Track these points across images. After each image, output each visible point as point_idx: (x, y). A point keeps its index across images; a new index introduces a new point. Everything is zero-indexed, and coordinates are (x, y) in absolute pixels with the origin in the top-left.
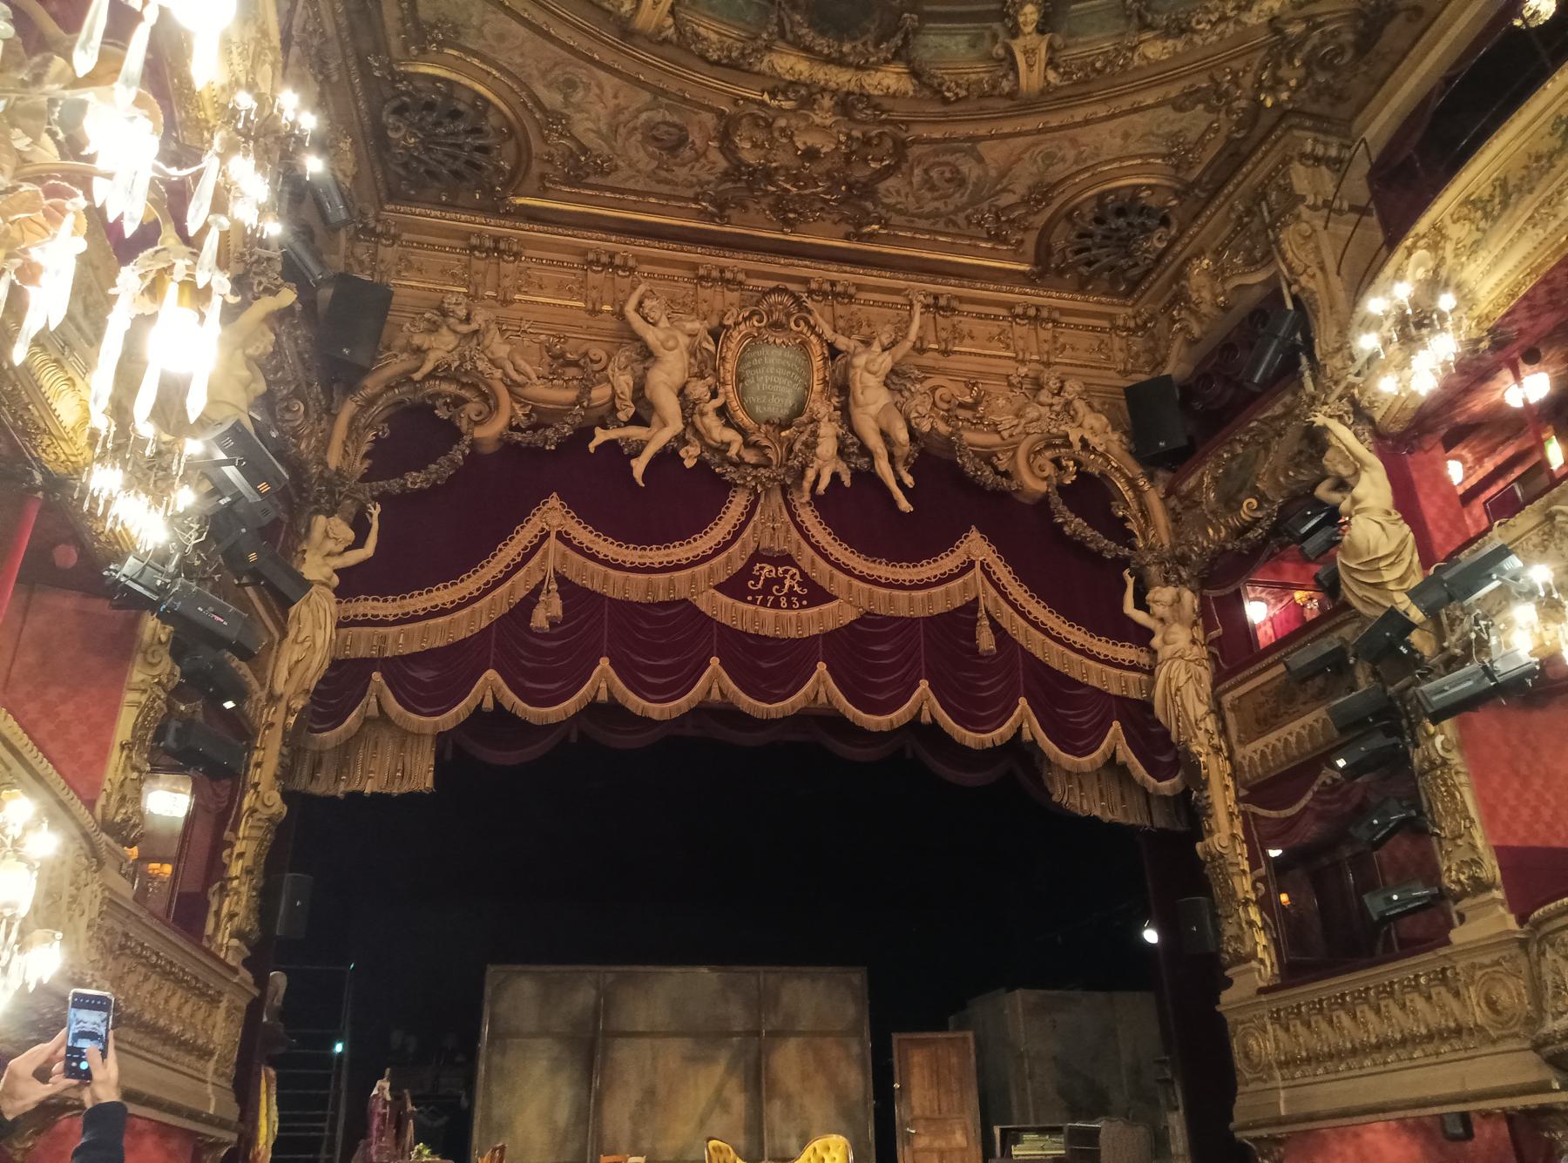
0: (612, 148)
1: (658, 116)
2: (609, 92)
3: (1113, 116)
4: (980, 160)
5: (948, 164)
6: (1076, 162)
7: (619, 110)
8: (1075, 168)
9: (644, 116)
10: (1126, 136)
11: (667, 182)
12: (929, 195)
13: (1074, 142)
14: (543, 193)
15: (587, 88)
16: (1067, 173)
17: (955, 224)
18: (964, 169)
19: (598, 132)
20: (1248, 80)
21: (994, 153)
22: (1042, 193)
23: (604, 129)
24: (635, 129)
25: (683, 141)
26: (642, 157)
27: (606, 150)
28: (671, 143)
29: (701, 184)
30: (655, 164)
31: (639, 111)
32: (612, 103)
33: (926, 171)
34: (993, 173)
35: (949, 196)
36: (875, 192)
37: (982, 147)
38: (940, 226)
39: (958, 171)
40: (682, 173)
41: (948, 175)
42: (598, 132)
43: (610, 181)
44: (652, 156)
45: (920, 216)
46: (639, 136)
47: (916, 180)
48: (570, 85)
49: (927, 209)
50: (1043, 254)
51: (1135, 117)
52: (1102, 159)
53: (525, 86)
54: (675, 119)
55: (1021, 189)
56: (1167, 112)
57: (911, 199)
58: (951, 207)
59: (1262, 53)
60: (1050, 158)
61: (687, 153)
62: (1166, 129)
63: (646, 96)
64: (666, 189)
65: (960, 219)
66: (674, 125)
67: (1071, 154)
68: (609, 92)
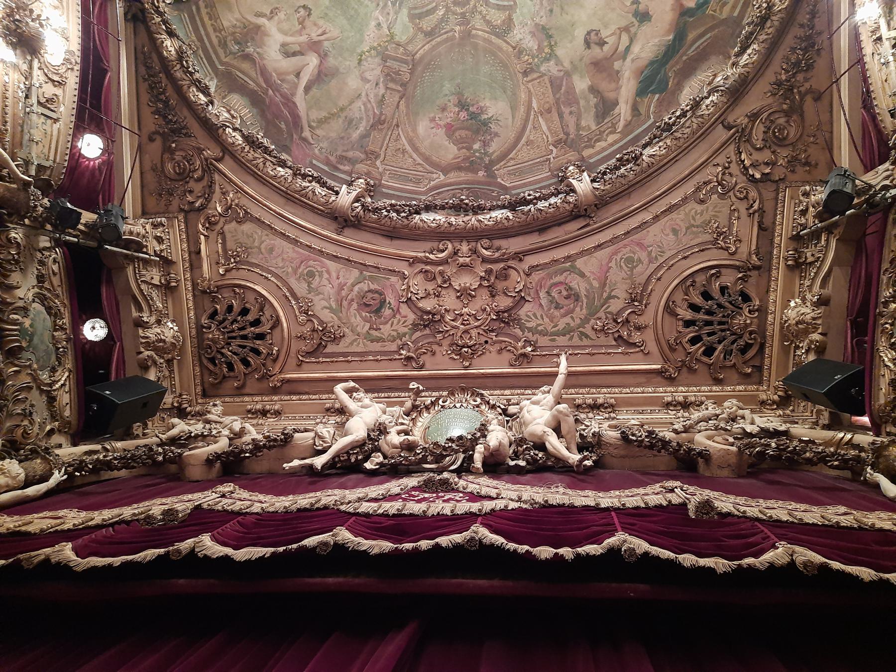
0: (340, 319)
2: (334, 275)
3: (656, 218)
4: (582, 275)
5: (561, 283)
6: (650, 262)
7: (341, 287)
9: (356, 288)
10: (675, 232)
11: (378, 340)
12: (557, 313)
13: (640, 245)
15: (321, 276)
16: (648, 272)
17: (587, 336)
18: (574, 284)
19: (330, 308)
20: (735, 169)
22: (638, 298)
24: (352, 300)
25: (383, 303)
26: (358, 321)
27: (337, 322)
28: (374, 305)
29: (400, 336)
30: (368, 325)
31: (353, 285)
32: (336, 283)
34: (596, 284)
35: (572, 311)
37: (579, 263)
38: (576, 341)
39: (571, 289)
41: (565, 293)
42: (330, 308)
43: (341, 347)
44: (365, 320)
45: (558, 334)
46: (355, 305)
47: (544, 302)
48: (311, 275)
49: (561, 326)
51: (674, 215)
52: (668, 254)
55: (621, 293)
56: (693, 207)
57: (546, 320)
58: (578, 321)
59: (731, 149)
60: (629, 260)
61: (387, 312)
62: (699, 220)
63: (355, 273)
64: (376, 347)
65: (588, 330)
66: (376, 292)
67: (643, 256)
68: (334, 275)
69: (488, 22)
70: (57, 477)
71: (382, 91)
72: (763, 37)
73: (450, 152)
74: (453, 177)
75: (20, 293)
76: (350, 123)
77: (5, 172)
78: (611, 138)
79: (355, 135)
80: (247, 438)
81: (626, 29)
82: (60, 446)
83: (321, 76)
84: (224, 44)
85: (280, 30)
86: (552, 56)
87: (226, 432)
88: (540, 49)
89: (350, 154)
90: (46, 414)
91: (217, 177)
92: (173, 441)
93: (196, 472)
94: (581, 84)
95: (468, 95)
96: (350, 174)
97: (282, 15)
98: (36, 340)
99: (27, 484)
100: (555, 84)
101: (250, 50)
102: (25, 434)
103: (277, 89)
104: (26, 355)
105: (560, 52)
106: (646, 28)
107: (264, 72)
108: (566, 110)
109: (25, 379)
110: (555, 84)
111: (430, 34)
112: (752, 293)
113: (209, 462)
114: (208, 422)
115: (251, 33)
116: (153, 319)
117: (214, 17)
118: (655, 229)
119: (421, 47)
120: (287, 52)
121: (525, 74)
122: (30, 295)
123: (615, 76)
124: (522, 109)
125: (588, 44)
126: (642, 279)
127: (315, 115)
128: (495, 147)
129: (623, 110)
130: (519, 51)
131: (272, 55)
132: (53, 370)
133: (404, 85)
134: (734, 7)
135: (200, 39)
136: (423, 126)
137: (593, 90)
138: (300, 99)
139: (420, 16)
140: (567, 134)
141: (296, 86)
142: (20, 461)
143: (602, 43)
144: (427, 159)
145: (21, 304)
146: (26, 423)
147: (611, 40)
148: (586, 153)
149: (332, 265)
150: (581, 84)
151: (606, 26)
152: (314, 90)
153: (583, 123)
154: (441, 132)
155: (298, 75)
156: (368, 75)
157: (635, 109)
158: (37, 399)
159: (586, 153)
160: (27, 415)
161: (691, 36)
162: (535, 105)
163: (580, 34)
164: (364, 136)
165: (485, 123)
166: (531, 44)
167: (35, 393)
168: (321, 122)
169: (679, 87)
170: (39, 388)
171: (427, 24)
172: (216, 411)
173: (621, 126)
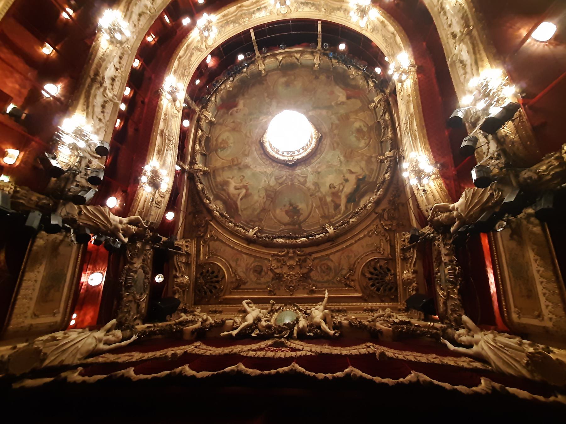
1: (256, 264)
3: (356, 242)
4: (332, 261)
6: (355, 256)
7: (247, 264)
8: (355, 259)
9: (253, 265)
10: (362, 246)
12: (324, 275)
14: (230, 293)
18: (329, 264)
20: (380, 226)
21: (334, 258)
22: (352, 269)
23: (244, 270)
25: (262, 270)
26: (253, 277)
28: (258, 271)
29: (268, 282)
33: (320, 267)
34: (337, 264)
36: (310, 277)
37: (331, 257)
38: (331, 285)
40: (263, 280)
43: (247, 286)
46: (252, 270)
49: (325, 279)
50: (364, 289)
51: (362, 241)
53: (228, 262)
54: (259, 264)
56: (367, 238)
58: (331, 278)
59: (378, 220)
61: (263, 273)
64: (259, 286)
65: (335, 281)
69: (299, 181)
70: (135, 337)
71: (265, 200)
72: (383, 187)
73: (286, 219)
74: (287, 227)
75: (135, 265)
76: (254, 210)
77: (140, 225)
78: (339, 216)
79: (256, 213)
80: (208, 323)
81: (342, 184)
82: (138, 324)
83: (246, 196)
84: (217, 186)
85: (235, 182)
86: (319, 191)
87: (200, 320)
88: (315, 188)
89: (254, 219)
90: (135, 312)
91: (209, 226)
92: (181, 323)
93: (187, 337)
94: (329, 199)
95: (293, 201)
96: (253, 225)
97: (235, 178)
98: (137, 283)
99: (122, 340)
100: (321, 199)
101: (225, 188)
102: (126, 320)
103: (232, 199)
104: (134, 288)
105: (321, 190)
106: (348, 184)
107: (228, 194)
108: (324, 207)
109: (130, 298)
110: (321, 199)
111: (281, 184)
112: (391, 268)
113: (193, 332)
114: (194, 315)
115: (226, 183)
116: (180, 275)
117: (215, 178)
118: (355, 245)
119: (278, 188)
120: (236, 188)
121: (311, 196)
122: (139, 266)
123: (340, 197)
124: (310, 207)
125: (330, 188)
126: (353, 262)
127: (243, 207)
128: (302, 218)
129: (343, 207)
130: (309, 189)
131: (231, 189)
132: (141, 294)
133: (272, 198)
134: (374, 178)
135: (210, 185)
136: (278, 211)
137: (332, 201)
138: (239, 203)
139: (278, 179)
140: (325, 214)
141: (238, 198)
142: (122, 331)
143: (335, 187)
144: (279, 221)
145: (135, 269)
146: (127, 315)
147: (337, 187)
148: (332, 220)
149: (244, 256)
150: (329, 199)
151: (336, 183)
152: (244, 200)
153: (330, 211)
154: (284, 213)
155: (239, 195)
156: (261, 196)
157: (346, 207)
158: (133, 306)
159: (332, 220)
160: (129, 312)
161: (362, 186)
162: (314, 205)
163: (328, 185)
164: (259, 214)
165: (299, 210)
166: (313, 187)
167: (133, 303)
168: (245, 209)
169: (359, 201)
170: (135, 301)
171: (280, 181)
172: (198, 311)
173: (342, 212)
